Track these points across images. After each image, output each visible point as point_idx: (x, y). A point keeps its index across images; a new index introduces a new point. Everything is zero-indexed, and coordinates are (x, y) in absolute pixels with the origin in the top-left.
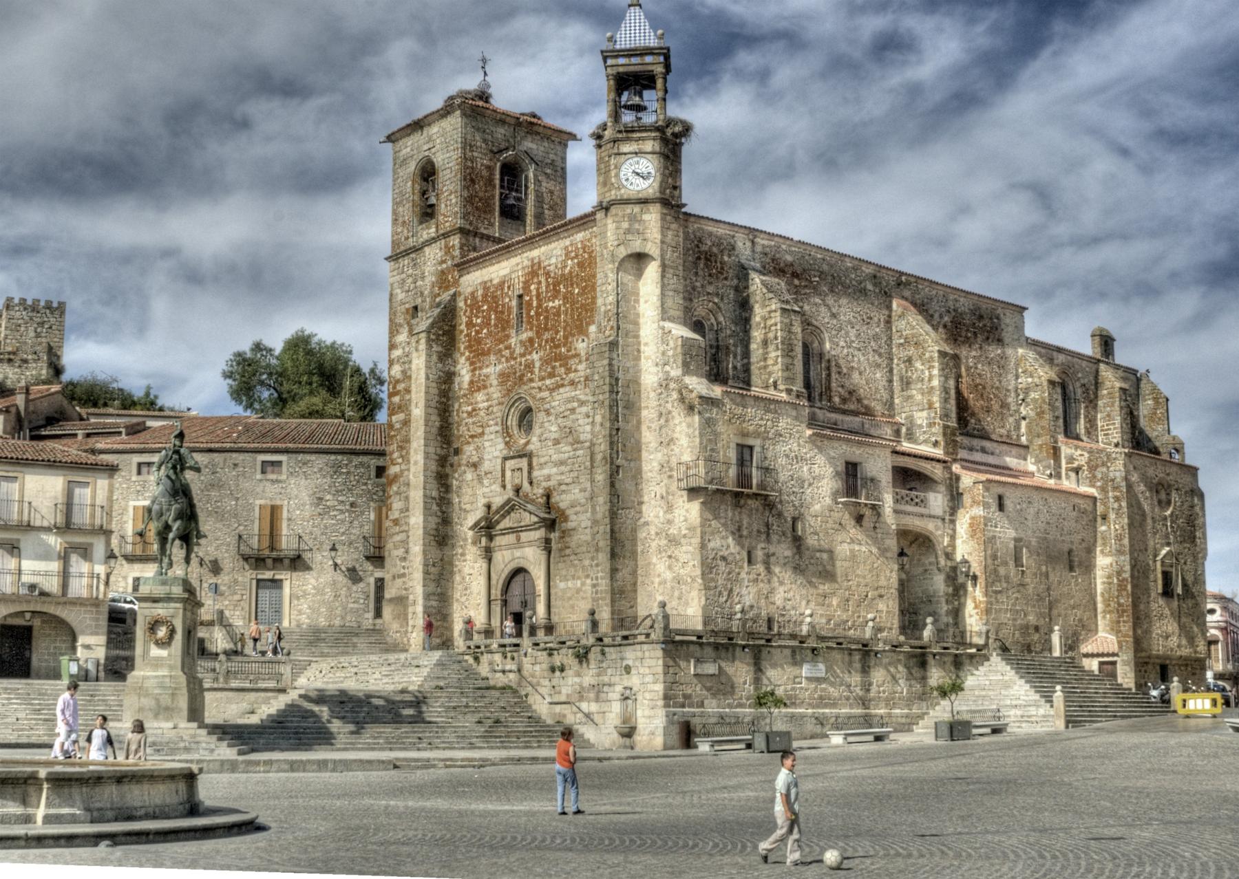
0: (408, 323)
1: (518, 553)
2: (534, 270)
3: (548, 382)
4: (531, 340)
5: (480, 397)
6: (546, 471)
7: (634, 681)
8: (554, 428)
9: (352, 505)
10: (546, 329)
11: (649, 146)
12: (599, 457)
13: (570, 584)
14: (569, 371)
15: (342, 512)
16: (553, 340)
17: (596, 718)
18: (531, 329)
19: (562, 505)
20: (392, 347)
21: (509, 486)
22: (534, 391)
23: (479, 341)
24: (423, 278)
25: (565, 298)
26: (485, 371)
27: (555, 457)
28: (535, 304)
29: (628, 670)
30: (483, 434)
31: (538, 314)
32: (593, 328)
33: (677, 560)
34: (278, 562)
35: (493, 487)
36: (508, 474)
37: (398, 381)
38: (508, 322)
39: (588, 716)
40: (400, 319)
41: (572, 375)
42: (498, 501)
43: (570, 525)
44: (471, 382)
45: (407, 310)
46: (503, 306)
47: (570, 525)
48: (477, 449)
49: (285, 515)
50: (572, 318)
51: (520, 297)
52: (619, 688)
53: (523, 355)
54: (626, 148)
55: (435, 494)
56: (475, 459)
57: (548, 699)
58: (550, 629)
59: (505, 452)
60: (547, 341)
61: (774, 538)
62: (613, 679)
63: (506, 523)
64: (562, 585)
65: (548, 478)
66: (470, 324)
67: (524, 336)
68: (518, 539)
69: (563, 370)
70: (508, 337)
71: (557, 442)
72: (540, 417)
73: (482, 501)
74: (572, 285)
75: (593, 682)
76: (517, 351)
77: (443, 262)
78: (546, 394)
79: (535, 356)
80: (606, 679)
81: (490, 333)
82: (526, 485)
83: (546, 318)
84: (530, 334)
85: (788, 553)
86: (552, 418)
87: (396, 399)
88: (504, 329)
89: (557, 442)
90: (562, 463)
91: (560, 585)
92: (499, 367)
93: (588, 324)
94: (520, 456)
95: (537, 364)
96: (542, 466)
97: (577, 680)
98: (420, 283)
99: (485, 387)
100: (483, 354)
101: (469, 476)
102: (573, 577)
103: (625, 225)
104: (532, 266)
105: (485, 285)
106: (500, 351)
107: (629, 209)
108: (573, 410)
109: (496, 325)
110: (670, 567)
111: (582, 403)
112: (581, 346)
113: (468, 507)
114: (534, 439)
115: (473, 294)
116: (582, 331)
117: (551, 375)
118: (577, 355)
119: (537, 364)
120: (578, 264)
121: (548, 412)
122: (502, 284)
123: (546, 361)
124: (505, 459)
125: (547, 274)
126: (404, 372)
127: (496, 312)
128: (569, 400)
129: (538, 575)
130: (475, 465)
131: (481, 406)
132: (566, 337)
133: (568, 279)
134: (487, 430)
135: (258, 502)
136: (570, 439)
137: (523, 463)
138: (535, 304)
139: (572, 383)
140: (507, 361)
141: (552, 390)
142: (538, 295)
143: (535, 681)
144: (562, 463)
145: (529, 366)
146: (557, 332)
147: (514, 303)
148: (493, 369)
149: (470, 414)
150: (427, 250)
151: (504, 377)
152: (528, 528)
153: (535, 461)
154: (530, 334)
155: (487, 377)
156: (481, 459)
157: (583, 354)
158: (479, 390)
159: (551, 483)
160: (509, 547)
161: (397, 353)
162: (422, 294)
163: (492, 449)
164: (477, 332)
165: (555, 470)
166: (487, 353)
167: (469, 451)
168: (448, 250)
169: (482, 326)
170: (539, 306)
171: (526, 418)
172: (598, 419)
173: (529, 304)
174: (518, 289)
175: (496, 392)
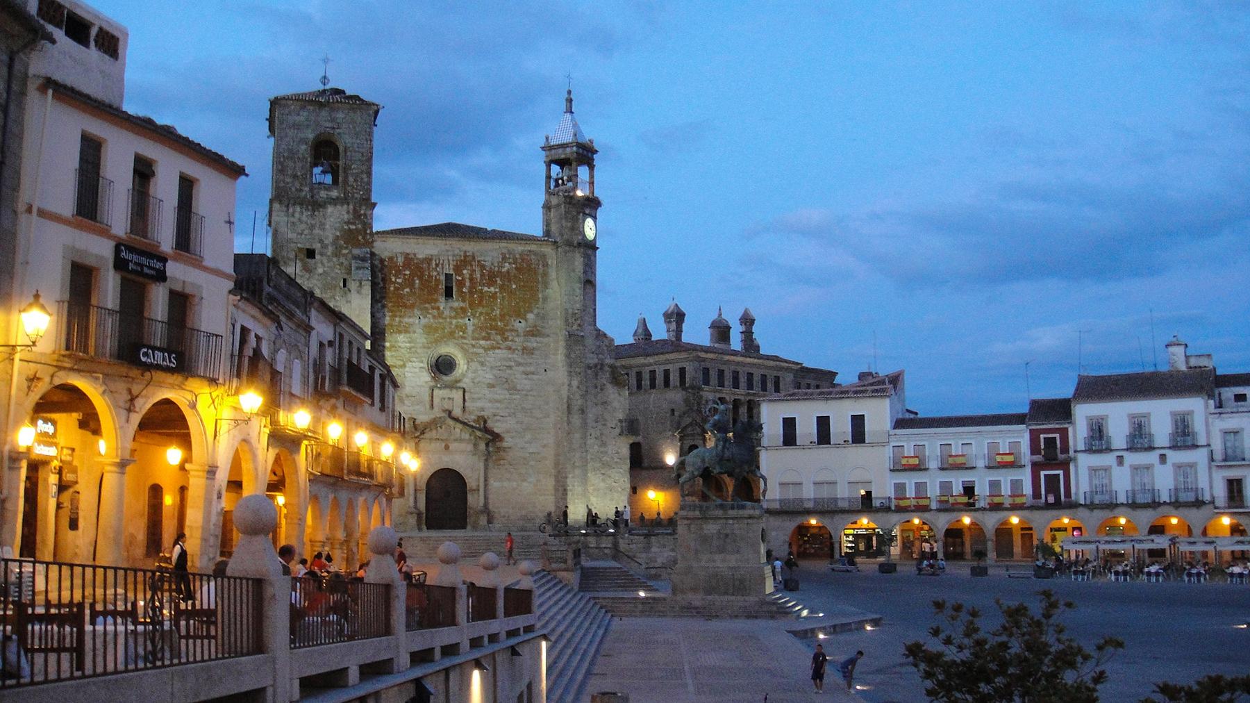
0: (301, 260)
2: (465, 261)
3: (482, 342)
4: (463, 310)
5: (401, 338)
6: (479, 404)
8: (489, 376)
12: (576, 408)
14: (506, 339)
16: (488, 314)
18: (463, 301)
19: (496, 430)
21: (436, 409)
23: (401, 297)
24: (324, 230)
25: (501, 287)
26: (406, 320)
27: (488, 396)
28: (468, 284)
30: (404, 366)
31: (471, 292)
32: (530, 316)
35: (417, 407)
38: (436, 289)
43: (505, 444)
45: (300, 250)
46: (430, 276)
47: (505, 444)
51: (448, 277)
53: (455, 318)
57: (644, 566)
58: (486, 510)
59: (432, 384)
60: (481, 313)
63: (433, 434)
65: (483, 409)
67: (456, 304)
68: (447, 447)
69: (499, 337)
70: (436, 301)
74: (509, 281)
76: (447, 313)
77: (348, 223)
78: (481, 351)
84: (462, 304)
88: (430, 293)
89: (491, 386)
91: (494, 484)
92: (424, 321)
93: (527, 312)
95: (470, 329)
97: (673, 554)
98: (317, 231)
99: (406, 332)
100: (405, 306)
102: (509, 480)
104: (466, 256)
106: (427, 309)
108: (510, 367)
109: (420, 289)
110: (603, 480)
111: (519, 364)
112: (521, 326)
114: (466, 380)
115: (391, 259)
116: (521, 315)
117: (484, 338)
119: (470, 329)
120: (516, 268)
121: (482, 364)
122: (428, 260)
125: (483, 267)
127: (420, 278)
128: (504, 359)
129: (473, 477)
131: (403, 345)
133: (507, 276)
136: (506, 386)
138: (468, 284)
139: (509, 348)
140: (434, 317)
142: (471, 279)
145: (463, 329)
146: (493, 310)
150: (330, 209)
152: (460, 440)
154: (462, 304)
155: (411, 325)
158: (400, 332)
159: (485, 414)
162: (321, 241)
164: (397, 289)
166: (412, 306)
168: (357, 215)
169: (402, 286)
172: (575, 383)
173: (461, 284)
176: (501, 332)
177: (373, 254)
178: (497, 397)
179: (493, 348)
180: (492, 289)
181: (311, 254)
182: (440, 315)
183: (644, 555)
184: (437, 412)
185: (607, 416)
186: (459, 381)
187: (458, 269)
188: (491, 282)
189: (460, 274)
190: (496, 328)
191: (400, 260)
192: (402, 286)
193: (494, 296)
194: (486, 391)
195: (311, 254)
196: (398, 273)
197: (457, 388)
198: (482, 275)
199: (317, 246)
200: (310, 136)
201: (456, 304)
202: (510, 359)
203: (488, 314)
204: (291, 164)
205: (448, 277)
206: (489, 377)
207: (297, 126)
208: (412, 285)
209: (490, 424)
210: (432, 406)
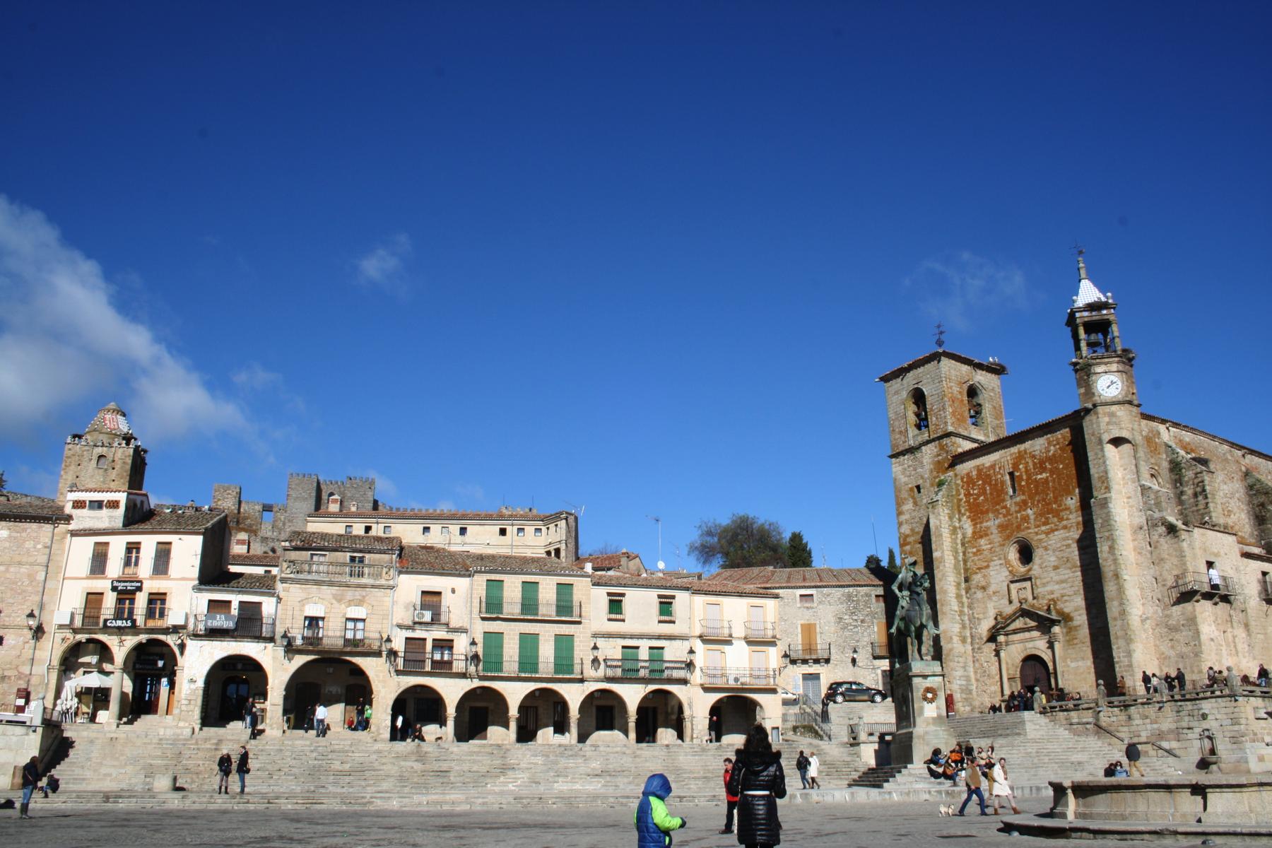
0: (913, 498)
1: (1030, 645)
2: (1020, 457)
3: (1043, 528)
4: (1024, 502)
5: (983, 541)
6: (1049, 588)
7: (1211, 724)
8: (1053, 559)
9: (862, 621)
10: (1037, 493)
11: (1114, 367)
12: (1111, 574)
13: (1080, 663)
14: (1061, 519)
15: (856, 627)
17: (1177, 752)
19: (1066, 610)
20: (900, 513)
22: (1032, 534)
23: (978, 505)
24: (922, 467)
25: (1052, 472)
27: (1056, 578)
29: (1204, 717)
30: (988, 567)
31: (1028, 484)
33: (1178, 641)
34: (817, 661)
36: (1014, 593)
37: (907, 536)
39: (1166, 751)
40: (904, 494)
41: (1065, 523)
42: (1009, 610)
44: (974, 533)
45: (911, 489)
47: (1075, 623)
48: (984, 576)
49: (818, 630)
50: (1059, 483)
52: (1198, 730)
54: (1099, 369)
55: (956, 608)
56: (983, 584)
59: (1010, 578)
61: (1235, 624)
62: (1192, 724)
64: (1073, 665)
65: (1052, 592)
66: (968, 495)
67: (1018, 499)
70: (1004, 500)
71: (1056, 568)
72: (1038, 555)
73: (992, 613)
75: (1173, 726)
76: (1013, 509)
78: (1043, 536)
79: (1029, 511)
80: (1185, 724)
81: (986, 500)
82: (1030, 598)
83: (1037, 487)
84: (1023, 497)
85: (1244, 635)
86: (1050, 552)
87: (908, 548)
88: (999, 496)
89: (1056, 568)
90: (1062, 582)
94: (1025, 580)
95: (1032, 517)
96: (1044, 585)
97: (1155, 726)
99: (987, 535)
100: (982, 513)
101: (979, 594)
103: (1107, 419)
105: (979, 469)
107: (1107, 409)
110: (1172, 647)
113: (981, 616)
114: (1036, 567)
115: (968, 474)
117: (1045, 524)
118: (1068, 509)
119: (1032, 517)
121: (1046, 549)
122: (993, 466)
123: (1039, 515)
124: (1012, 582)
125: (1034, 457)
126: (912, 530)
127: (990, 485)
128: (1064, 539)
130: (984, 588)
132: (1055, 498)
133: (1052, 460)
134: (992, 564)
135: (800, 622)
136: (1069, 565)
137: (1028, 584)
139: (1065, 527)
141: (1047, 533)
142: (1027, 471)
143: (1112, 729)
144: (1062, 582)
145: (1026, 519)
147: (1008, 477)
148: (992, 523)
149: (975, 554)
151: (1002, 528)
153: (1038, 582)
154: (1023, 497)
155: (988, 528)
156: (989, 584)
157: (1072, 507)
158: (981, 537)
160: (1022, 641)
161: (903, 518)
162: (922, 477)
163: (998, 576)
165: (1056, 587)
166: (987, 512)
167: (977, 579)
168: (942, 448)
169: (979, 495)
170: (1029, 478)
171: (1026, 554)
173: (1020, 477)
174: (1009, 468)
175: (996, 537)
176: (1057, 514)
177: (956, 475)
178: (1062, 577)
179: (1053, 531)
180: (1044, 475)
181: (918, 487)
182: (1008, 513)
183: (1125, 729)
184: (1016, 605)
185: (1165, 574)
186: (1030, 570)
187: (1015, 466)
188: (1043, 470)
189: (1018, 470)
190: (1051, 511)
191: (974, 473)
192: (979, 495)
193: (1046, 480)
194: (1052, 574)
195: (918, 487)
196: (974, 484)
197: (1030, 579)
198: (1035, 464)
199: (920, 482)
200: (904, 394)
201: (1018, 499)
202: (1067, 538)
203: (1044, 500)
204: (897, 423)
205: (1011, 474)
206: (1052, 559)
207: (897, 393)
208: (984, 493)
209: (1060, 605)
210: (1011, 602)
